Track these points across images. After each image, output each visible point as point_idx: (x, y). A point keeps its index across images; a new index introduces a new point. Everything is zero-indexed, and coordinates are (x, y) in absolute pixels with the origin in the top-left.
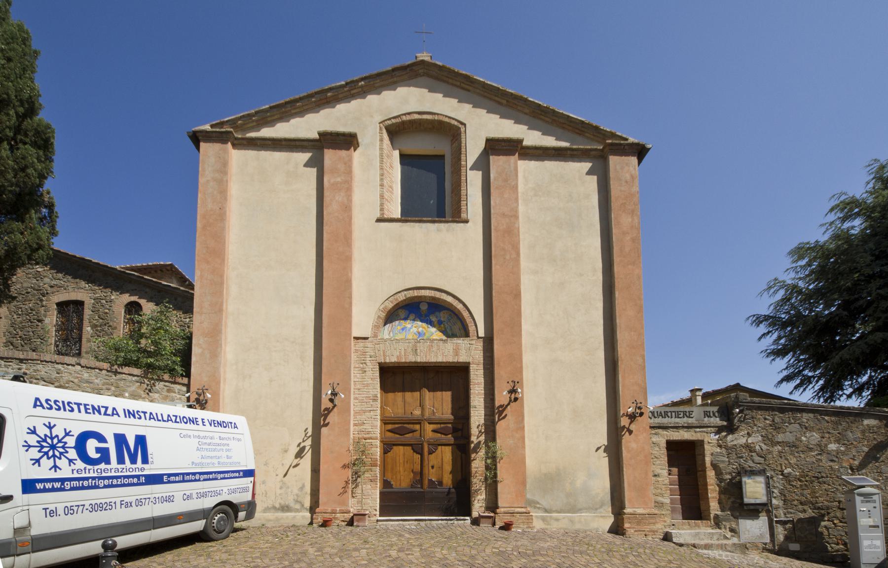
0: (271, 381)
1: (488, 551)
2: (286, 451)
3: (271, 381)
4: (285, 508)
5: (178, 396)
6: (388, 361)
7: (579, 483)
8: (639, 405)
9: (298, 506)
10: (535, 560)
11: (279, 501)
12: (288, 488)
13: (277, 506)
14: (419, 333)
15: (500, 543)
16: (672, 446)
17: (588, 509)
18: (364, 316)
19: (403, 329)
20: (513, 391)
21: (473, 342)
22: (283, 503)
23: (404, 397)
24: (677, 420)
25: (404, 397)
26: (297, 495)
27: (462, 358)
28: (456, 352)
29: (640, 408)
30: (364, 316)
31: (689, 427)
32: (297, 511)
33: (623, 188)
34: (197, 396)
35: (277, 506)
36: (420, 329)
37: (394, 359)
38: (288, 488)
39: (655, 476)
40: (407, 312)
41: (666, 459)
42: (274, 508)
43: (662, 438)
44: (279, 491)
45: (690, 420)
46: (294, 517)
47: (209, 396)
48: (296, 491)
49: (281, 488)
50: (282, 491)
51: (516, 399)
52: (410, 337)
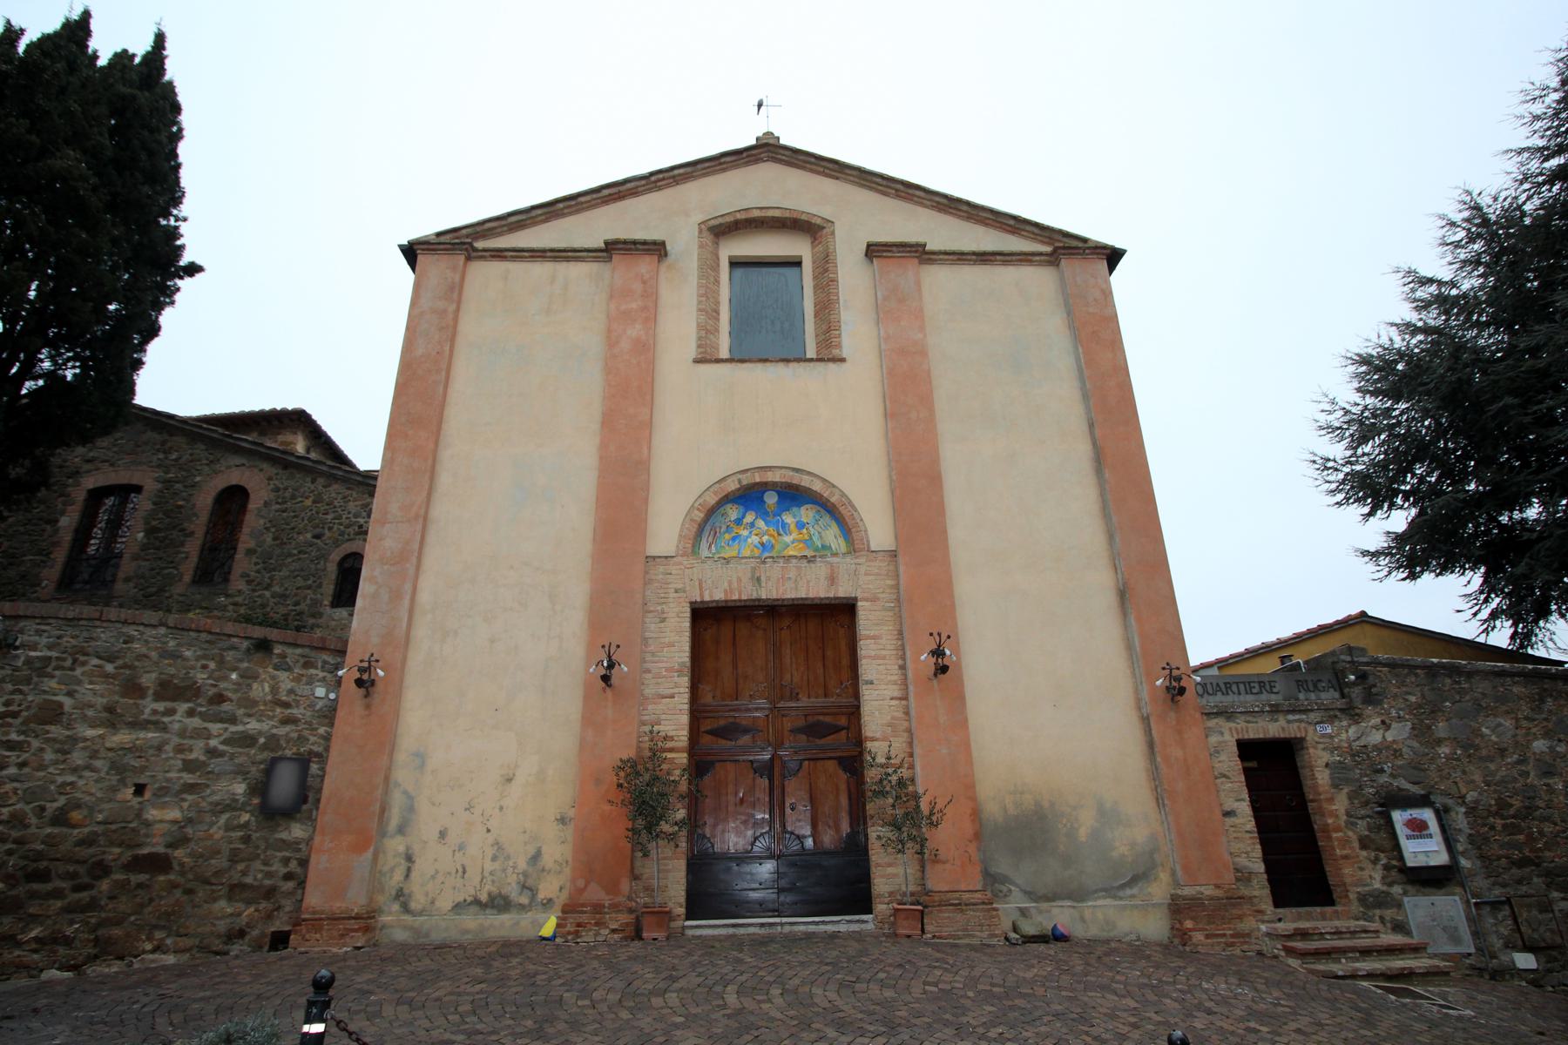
0: (492, 641)
1: (917, 990)
2: (509, 780)
3: (492, 641)
4: (499, 903)
5: (321, 674)
6: (707, 598)
7: (1083, 834)
8: (1175, 673)
9: (524, 900)
10: (1012, 1008)
11: (488, 887)
12: (508, 858)
13: (484, 897)
14: (762, 544)
15: (938, 973)
16: (1246, 749)
17: (1110, 892)
18: (666, 528)
19: (734, 539)
20: (938, 653)
21: (862, 560)
22: (494, 890)
23: (702, 595)
24: (1250, 698)
25: (702, 595)
26: (525, 874)
27: (843, 591)
28: (832, 580)
29: (1178, 679)
30: (666, 528)
31: (1275, 710)
32: (522, 908)
33: (1091, 310)
34: (358, 675)
35: (484, 897)
36: (765, 538)
37: (719, 596)
38: (508, 858)
39: (1227, 814)
40: (742, 509)
41: (1243, 778)
42: (477, 902)
43: (1227, 736)
44: (489, 866)
45: (1274, 699)
46: (517, 924)
47: (381, 673)
48: (522, 865)
49: (494, 859)
50: (497, 865)
51: (943, 669)
52: (746, 553)
